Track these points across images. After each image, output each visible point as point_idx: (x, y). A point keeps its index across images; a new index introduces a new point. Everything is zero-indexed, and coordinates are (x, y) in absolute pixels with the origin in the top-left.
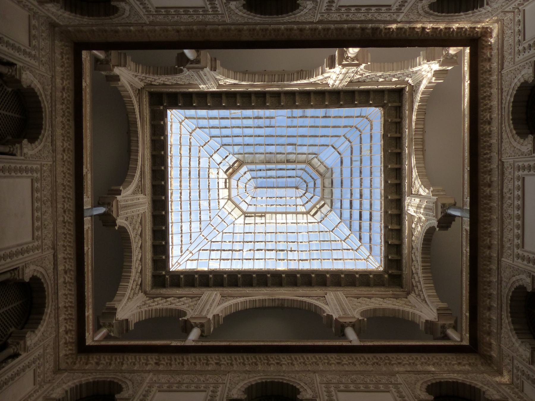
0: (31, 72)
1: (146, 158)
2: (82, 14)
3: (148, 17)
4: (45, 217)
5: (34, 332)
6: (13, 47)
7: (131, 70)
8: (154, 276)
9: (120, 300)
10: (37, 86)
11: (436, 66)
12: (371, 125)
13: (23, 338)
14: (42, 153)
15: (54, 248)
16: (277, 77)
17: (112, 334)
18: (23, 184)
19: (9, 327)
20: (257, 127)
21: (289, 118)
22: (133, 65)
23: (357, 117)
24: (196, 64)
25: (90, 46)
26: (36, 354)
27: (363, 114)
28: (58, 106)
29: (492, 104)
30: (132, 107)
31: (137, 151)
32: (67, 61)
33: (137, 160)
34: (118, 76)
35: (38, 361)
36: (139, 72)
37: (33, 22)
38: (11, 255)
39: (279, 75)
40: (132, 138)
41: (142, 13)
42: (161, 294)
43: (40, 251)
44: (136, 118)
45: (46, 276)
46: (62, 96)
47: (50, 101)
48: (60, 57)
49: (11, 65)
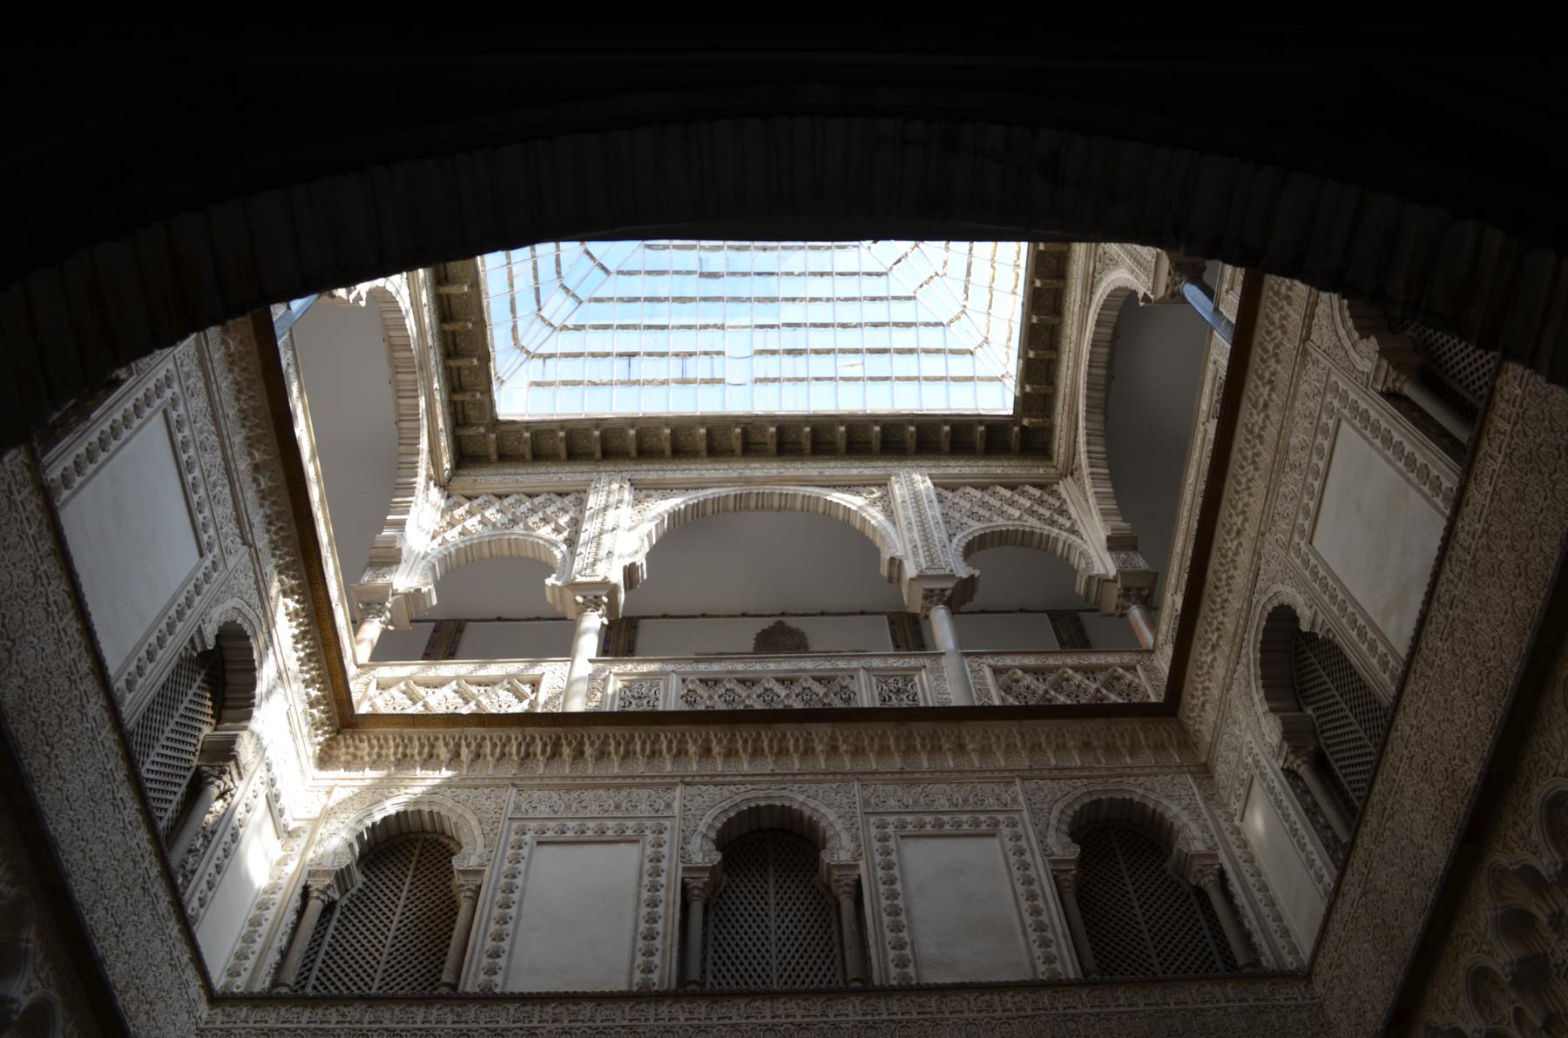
1: (1076, 318)
3: (1015, 800)
6: (1279, 804)
11: (403, 580)
12: (515, 338)
15: (1305, 352)
16: (753, 504)
20: (798, 325)
21: (719, 353)
22: (1074, 558)
23: (551, 356)
24: (932, 591)
25: (1145, 711)
27: (538, 362)
28: (1231, 628)
29: (261, 512)
30: (1093, 448)
31: (1095, 343)
33: (1098, 323)
38: (1387, 440)
39: (747, 508)
40: (1102, 372)
41: (1025, 814)
43: (1333, 378)
44: (1087, 420)
46: (1220, 637)
48: (1208, 706)
49: (1290, 774)
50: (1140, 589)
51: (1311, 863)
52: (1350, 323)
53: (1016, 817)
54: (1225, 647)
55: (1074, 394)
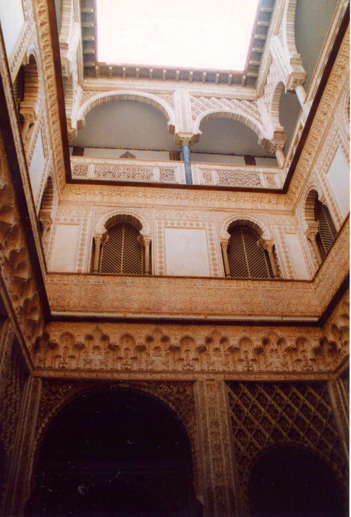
0: (95, 224)
8: (245, 85)
9: (259, 130)
13: (264, 241)
15: (212, 211)
17: (282, 146)
18: (169, 233)
26: (277, 231)
31: (137, 96)
33: (145, 98)
35: (282, 230)
38: (213, 249)
40: (125, 99)
42: (261, 86)
43: (212, 223)
45: (229, 219)
48: (80, 196)
55: (116, 89)
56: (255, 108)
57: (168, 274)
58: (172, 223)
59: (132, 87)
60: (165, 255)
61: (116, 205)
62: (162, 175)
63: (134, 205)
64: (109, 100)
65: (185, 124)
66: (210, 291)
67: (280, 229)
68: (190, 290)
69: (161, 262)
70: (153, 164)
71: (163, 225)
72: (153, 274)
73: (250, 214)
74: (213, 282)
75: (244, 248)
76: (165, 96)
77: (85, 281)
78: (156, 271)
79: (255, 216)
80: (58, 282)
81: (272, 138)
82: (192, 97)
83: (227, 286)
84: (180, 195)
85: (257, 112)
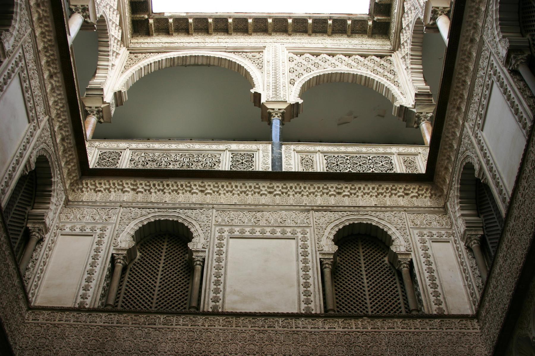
0: (118, 235)
2: (50, 184)
3: (41, 121)
4: (272, 222)
5: (393, 241)
7: (106, 77)
9: (393, 95)
10: (132, 227)
13: (395, 255)
14: (203, 223)
15: (308, 211)
18: (236, 249)
19: (383, 264)
24: (88, 10)
26: (418, 238)
28: (153, 200)
30: (153, 65)
32: (103, 185)
33: (220, 59)
34: (115, 93)
36: (108, 66)
37: (67, 230)
38: (306, 269)
40: (192, 62)
43: (308, 230)
45: (337, 222)
47: (148, 210)
48: (100, 194)
49: (113, 260)
50: (102, 117)
51: (86, 289)
52: (334, 232)
53: (37, 128)
54: (140, 197)
56: (389, 66)
57: (228, 308)
58: (242, 232)
59: (202, 45)
60: (225, 280)
61: (156, 205)
62: (234, 161)
63: (183, 206)
64: (168, 65)
65: (276, 89)
66: (296, 336)
67: (421, 235)
68: (261, 335)
69: (217, 291)
70: (222, 147)
71: (226, 234)
72: (201, 310)
73: (373, 214)
74: (301, 322)
75: (363, 269)
76: (250, 55)
77: (88, 321)
78: (208, 305)
79: (381, 217)
80: (45, 322)
81: (414, 104)
82: (292, 55)
83: (327, 327)
84: (259, 188)
85: (392, 72)
